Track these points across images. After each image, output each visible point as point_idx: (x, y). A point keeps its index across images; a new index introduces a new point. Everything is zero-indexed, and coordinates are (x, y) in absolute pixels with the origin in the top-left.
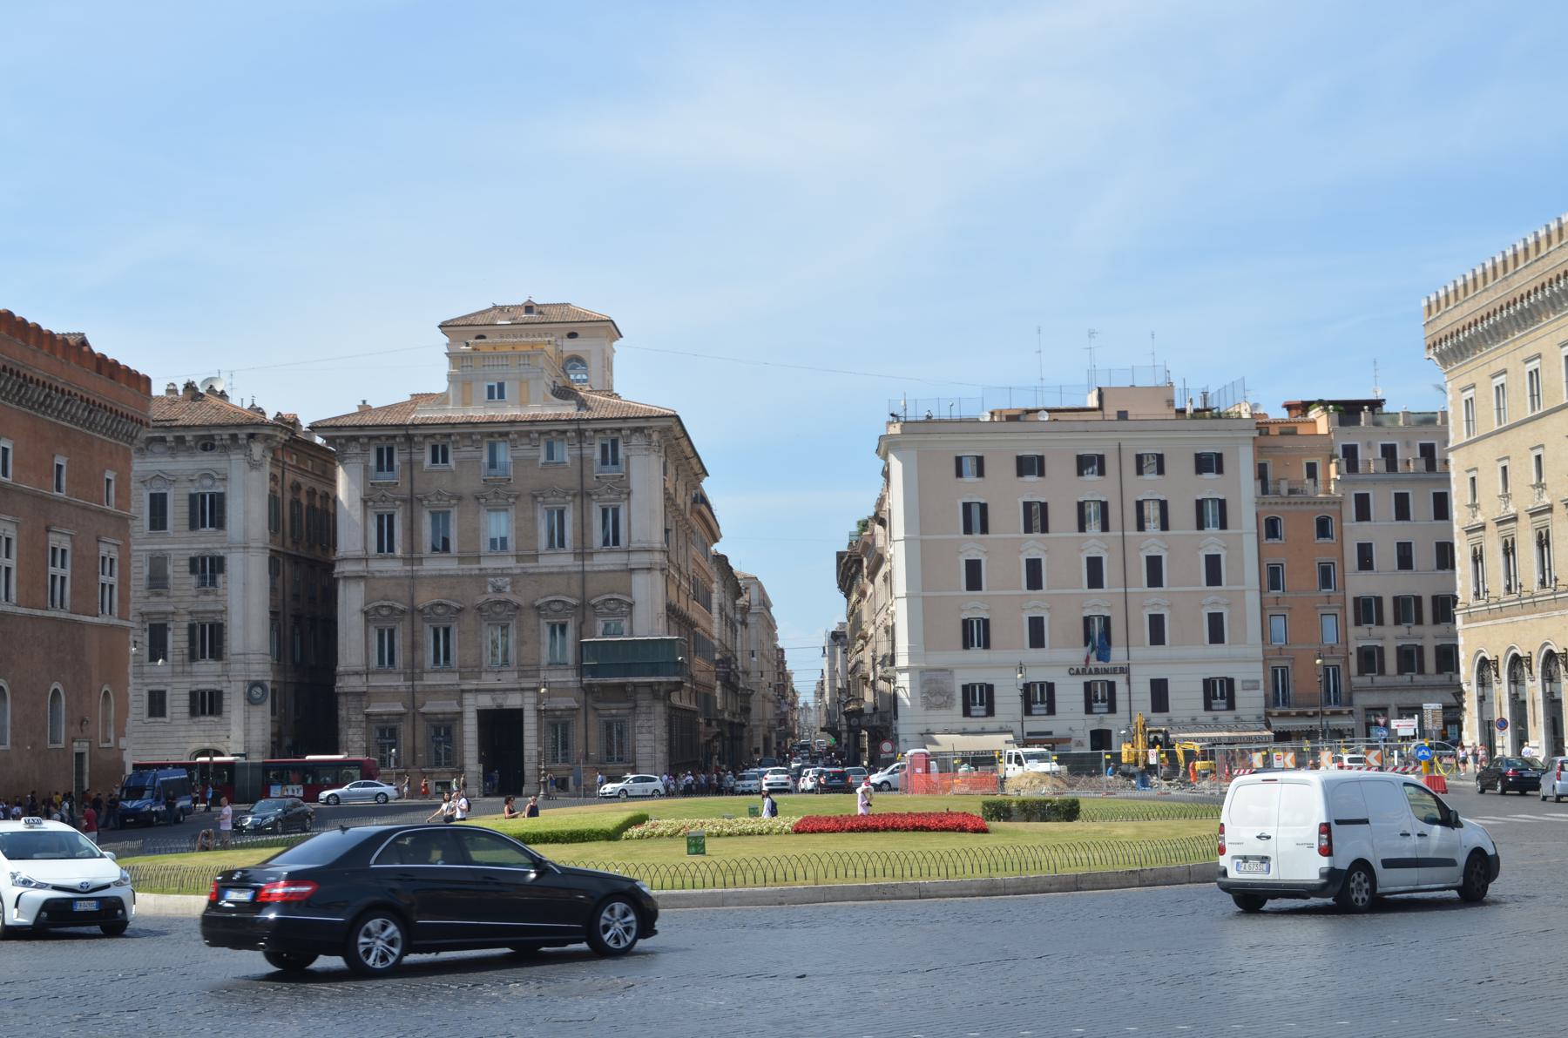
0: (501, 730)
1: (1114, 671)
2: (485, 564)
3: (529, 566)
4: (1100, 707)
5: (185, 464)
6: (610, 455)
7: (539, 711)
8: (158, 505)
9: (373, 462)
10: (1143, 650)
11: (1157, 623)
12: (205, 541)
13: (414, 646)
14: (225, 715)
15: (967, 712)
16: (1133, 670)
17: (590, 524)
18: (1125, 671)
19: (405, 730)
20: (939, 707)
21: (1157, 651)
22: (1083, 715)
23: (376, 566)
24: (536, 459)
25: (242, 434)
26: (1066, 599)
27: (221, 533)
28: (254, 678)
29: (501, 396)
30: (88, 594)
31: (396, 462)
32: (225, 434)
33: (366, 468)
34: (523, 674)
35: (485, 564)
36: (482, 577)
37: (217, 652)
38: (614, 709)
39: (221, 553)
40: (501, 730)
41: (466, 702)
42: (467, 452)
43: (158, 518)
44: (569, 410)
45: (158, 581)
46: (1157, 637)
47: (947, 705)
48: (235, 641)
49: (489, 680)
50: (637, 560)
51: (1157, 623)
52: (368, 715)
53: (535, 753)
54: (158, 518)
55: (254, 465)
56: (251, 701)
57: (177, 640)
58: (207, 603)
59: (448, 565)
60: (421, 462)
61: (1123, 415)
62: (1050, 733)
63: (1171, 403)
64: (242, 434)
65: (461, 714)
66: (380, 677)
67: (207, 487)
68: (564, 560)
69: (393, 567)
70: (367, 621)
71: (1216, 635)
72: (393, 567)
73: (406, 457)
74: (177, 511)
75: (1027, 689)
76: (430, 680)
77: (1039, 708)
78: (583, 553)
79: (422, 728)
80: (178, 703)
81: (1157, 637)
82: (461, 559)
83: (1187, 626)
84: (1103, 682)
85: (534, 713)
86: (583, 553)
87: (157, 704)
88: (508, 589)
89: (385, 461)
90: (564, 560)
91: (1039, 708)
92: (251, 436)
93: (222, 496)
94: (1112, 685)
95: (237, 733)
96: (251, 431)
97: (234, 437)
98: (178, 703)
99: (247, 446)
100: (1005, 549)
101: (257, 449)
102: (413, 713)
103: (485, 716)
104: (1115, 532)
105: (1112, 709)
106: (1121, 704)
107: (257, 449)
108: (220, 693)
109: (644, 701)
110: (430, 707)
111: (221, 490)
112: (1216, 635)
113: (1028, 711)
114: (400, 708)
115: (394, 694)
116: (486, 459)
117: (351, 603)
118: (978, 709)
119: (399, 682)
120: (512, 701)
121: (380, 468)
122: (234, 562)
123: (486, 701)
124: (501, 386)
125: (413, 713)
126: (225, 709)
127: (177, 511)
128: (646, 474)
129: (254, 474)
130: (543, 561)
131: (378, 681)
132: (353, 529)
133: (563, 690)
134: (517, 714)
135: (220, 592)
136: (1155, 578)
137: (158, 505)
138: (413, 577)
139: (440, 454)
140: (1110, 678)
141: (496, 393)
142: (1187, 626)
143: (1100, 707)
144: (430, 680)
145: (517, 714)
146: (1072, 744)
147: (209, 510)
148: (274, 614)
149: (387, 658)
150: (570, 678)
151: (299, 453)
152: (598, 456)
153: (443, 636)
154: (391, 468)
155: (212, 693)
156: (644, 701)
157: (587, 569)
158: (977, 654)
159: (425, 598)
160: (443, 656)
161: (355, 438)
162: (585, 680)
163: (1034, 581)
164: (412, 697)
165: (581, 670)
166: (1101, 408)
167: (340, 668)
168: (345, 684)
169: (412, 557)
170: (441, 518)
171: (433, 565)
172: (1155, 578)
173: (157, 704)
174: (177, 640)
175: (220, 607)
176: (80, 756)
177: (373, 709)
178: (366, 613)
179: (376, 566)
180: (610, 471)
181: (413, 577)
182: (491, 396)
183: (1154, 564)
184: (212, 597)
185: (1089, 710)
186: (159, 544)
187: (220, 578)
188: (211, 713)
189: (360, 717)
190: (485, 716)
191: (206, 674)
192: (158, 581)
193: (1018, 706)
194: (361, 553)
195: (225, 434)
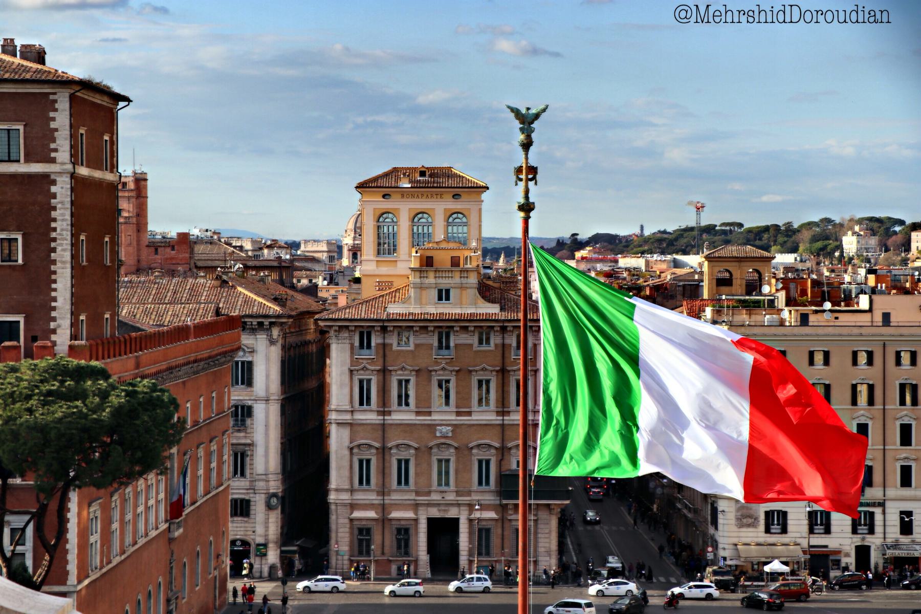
0: (443, 531)
1: (874, 505)
2: (435, 417)
3: (464, 419)
4: (863, 529)
9: (357, 344)
10: (896, 490)
11: (906, 472)
13: (383, 472)
14: (252, 516)
15: (768, 530)
16: (888, 504)
17: (508, 392)
18: (882, 505)
20: (749, 526)
21: (906, 492)
22: (850, 535)
23: (359, 416)
24: (471, 345)
25: (266, 322)
27: (249, 389)
28: (272, 491)
29: (448, 299)
31: (373, 344)
32: (255, 322)
33: (352, 345)
34: (458, 493)
35: (435, 417)
39: (250, 403)
40: (443, 531)
41: (420, 512)
42: (424, 339)
44: (493, 309)
46: (906, 480)
47: (753, 525)
49: (435, 497)
51: (906, 472)
52: (351, 520)
53: (467, 549)
55: (272, 342)
56: (269, 507)
58: (239, 438)
60: (391, 345)
61: (886, 317)
62: (826, 547)
64: (266, 322)
66: (360, 493)
69: (370, 417)
70: (351, 454)
72: (370, 417)
73: (380, 341)
76: (395, 497)
77: (819, 529)
81: (906, 480)
82: (418, 413)
84: (865, 513)
85: (466, 522)
88: (450, 434)
89: (365, 343)
91: (819, 529)
92: (271, 324)
93: (250, 364)
94: (872, 514)
95: (260, 530)
96: (273, 320)
97: (261, 324)
99: (269, 329)
101: (275, 332)
102: (384, 521)
103: (431, 521)
104: (878, 406)
105: (871, 531)
106: (878, 529)
107: (275, 332)
108: (248, 502)
110: (395, 515)
111: (250, 359)
113: (811, 531)
114: (372, 514)
116: (436, 344)
118: (775, 528)
119: (373, 497)
120: (452, 513)
121: (361, 346)
122: (259, 410)
123: (435, 513)
124: (448, 291)
125: (384, 521)
126: (252, 512)
129: (273, 348)
130: (475, 417)
131: (360, 497)
135: (248, 431)
136: (906, 439)
140: (871, 509)
141: (444, 295)
143: (863, 529)
144: (395, 497)
146: (842, 554)
148: (282, 443)
149: (364, 479)
152: (514, 344)
154: (369, 347)
155: (242, 500)
157: (506, 422)
160: (403, 478)
161: (347, 327)
162: (504, 502)
164: (383, 508)
166: (870, 310)
167: (333, 484)
169: (384, 411)
171: (401, 416)
172: (906, 439)
175: (248, 441)
177: (357, 514)
178: (351, 449)
179: (359, 416)
181: (383, 426)
182: (440, 299)
183: (906, 431)
184: (242, 434)
185: (854, 531)
187: (248, 421)
188: (242, 515)
189: (347, 521)
190: (431, 521)
193: (805, 528)
194: (348, 408)
195: (255, 322)
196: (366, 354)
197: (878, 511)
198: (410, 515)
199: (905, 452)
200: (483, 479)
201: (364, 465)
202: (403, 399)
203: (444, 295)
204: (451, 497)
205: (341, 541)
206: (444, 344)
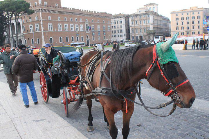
5: (119, 19)
6: (148, 16)
7: (144, 36)
8: (118, 22)
12: (121, 24)
13: (135, 31)
19: (134, 37)
21: (193, 29)
26: (185, 25)
30: (107, 29)
36: (139, 26)
37: (122, 32)
38: (149, 35)
40: (141, 37)
42: (138, 16)
43: (118, 23)
45: (118, 28)
48: (123, 31)
49: (140, 33)
50: (150, 24)
54: (118, 23)
57: (119, 32)
59: (137, 25)
63: (197, 8)
65: (138, 36)
67: (121, 21)
68: (145, 24)
69: (133, 25)
71: (199, 28)
74: (119, 22)
75: (182, 33)
78: (146, 24)
79: (136, 37)
80: (120, 36)
83: (196, 27)
86: (146, 24)
87: (118, 36)
89: (132, 18)
90: (145, 24)
94: (189, 32)
98: (120, 36)
100: (180, 22)
101: (124, 18)
103: (140, 36)
109: (151, 35)
112: (199, 28)
115: (133, 35)
117: (130, 28)
119: (134, 34)
120: (142, 35)
123: (140, 35)
127: (119, 22)
128: (151, 17)
131: (133, 34)
132: (130, 23)
133: (145, 34)
134: (142, 36)
137: (118, 22)
138: (135, 26)
139: (136, 17)
142: (196, 27)
145: (142, 36)
147: (121, 22)
148: (126, 29)
150: (146, 33)
151: (127, 17)
153: (137, 30)
156: (151, 35)
158: (177, 30)
159: (135, 28)
163: (182, 24)
165: (147, 32)
168: (130, 34)
169: (135, 25)
170: (136, 22)
171: (136, 25)
173: (118, 36)
174: (119, 32)
176: (107, 40)
180: (149, 17)
186: (118, 25)
190: (140, 36)
191: (121, 34)
192: (118, 28)
196: (133, 19)
197: (190, 32)
198: (137, 36)
199: (193, 24)
200: (145, 31)
201: (133, 30)
202: (136, 23)
203: (140, 12)
204: (141, 33)
205: (131, 38)
206: (140, 17)
